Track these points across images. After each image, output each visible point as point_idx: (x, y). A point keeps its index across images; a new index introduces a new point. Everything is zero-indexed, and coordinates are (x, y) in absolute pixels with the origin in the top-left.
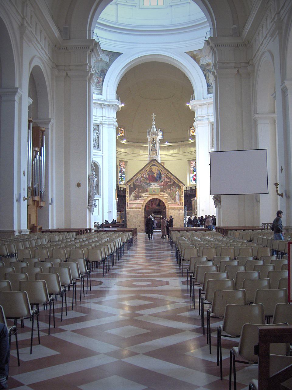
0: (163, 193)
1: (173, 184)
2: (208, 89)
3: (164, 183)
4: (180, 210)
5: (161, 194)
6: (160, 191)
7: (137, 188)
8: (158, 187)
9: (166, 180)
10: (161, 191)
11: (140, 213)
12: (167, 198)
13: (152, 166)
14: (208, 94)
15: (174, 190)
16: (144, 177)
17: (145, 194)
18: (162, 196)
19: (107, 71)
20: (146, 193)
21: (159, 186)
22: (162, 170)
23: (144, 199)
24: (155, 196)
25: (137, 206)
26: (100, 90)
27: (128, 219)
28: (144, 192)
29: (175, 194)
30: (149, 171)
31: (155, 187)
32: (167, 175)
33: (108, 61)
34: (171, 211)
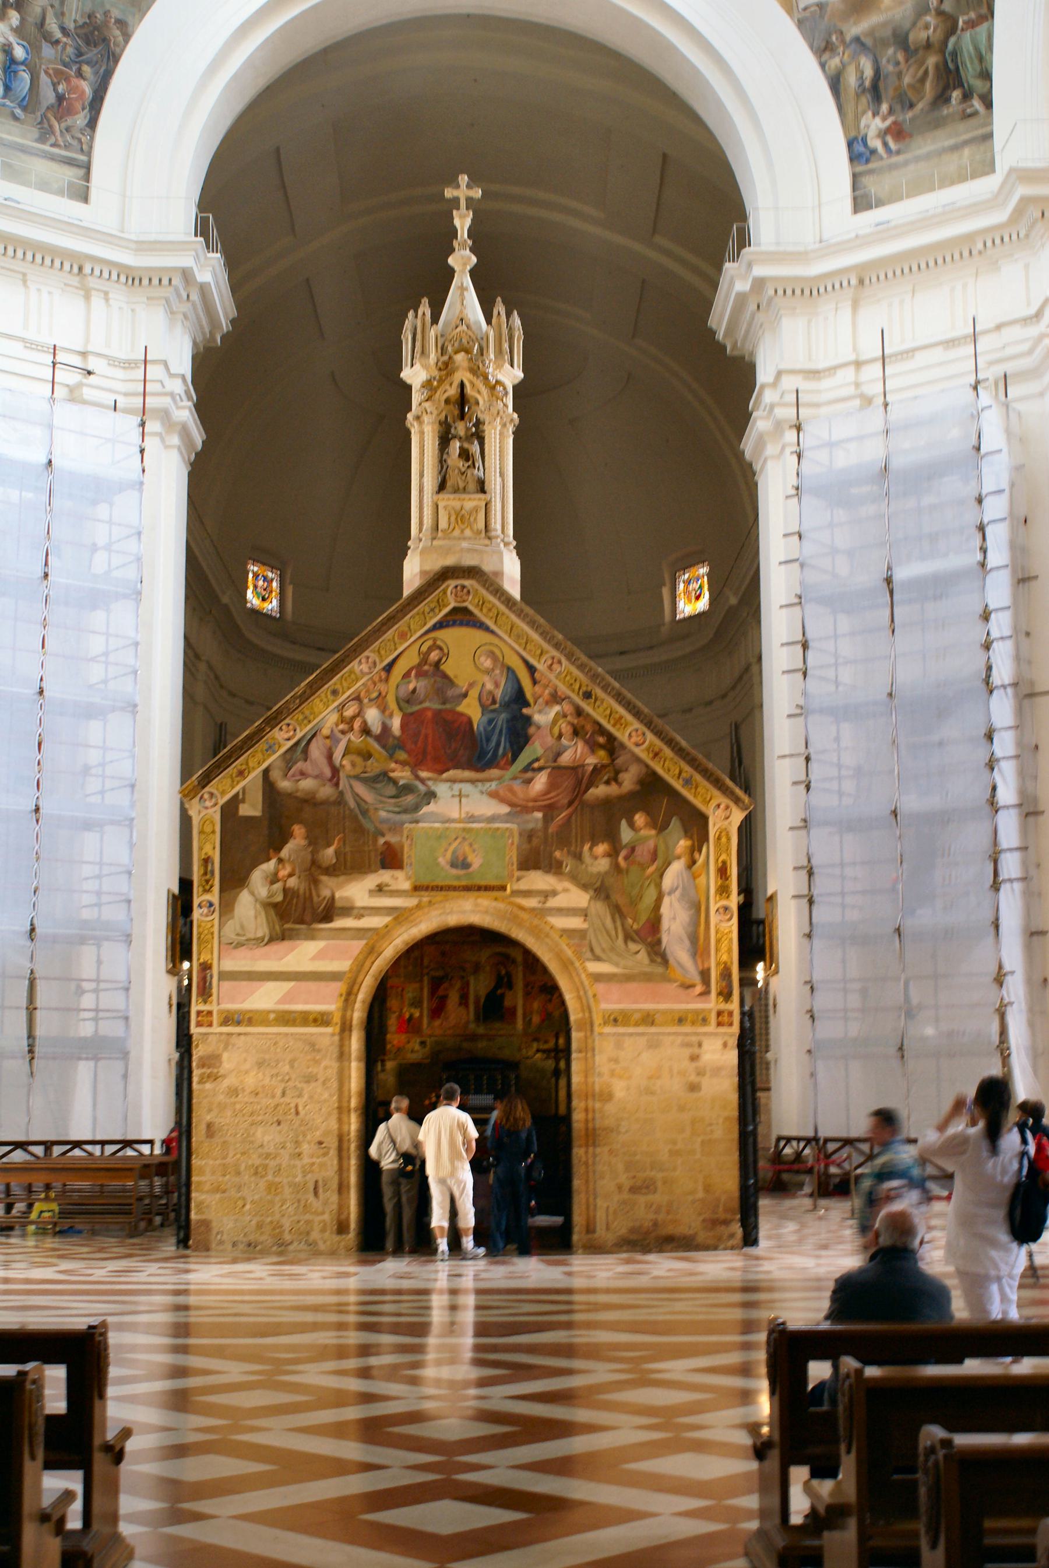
0: (538, 880)
1: (631, 795)
2: (855, 177)
3: (552, 785)
4: (706, 1046)
5: (523, 885)
6: (513, 856)
7: (298, 830)
8: (492, 819)
9: (574, 752)
10: (530, 861)
11: (328, 1066)
12: (575, 923)
13: (440, 626)
14: (861, 203)
15: (642, 853)
16: (366, 731)
17: (372, 881)
18: (532, 903)
19: (127, 37)
20: (385, 876)
21: (505, 809)
22: (531, 669)
23: (360, 933)
25: (286, 998)
26: (70, 162)
29: (659, 886)
31: (472, 818)
32: (579, 712)
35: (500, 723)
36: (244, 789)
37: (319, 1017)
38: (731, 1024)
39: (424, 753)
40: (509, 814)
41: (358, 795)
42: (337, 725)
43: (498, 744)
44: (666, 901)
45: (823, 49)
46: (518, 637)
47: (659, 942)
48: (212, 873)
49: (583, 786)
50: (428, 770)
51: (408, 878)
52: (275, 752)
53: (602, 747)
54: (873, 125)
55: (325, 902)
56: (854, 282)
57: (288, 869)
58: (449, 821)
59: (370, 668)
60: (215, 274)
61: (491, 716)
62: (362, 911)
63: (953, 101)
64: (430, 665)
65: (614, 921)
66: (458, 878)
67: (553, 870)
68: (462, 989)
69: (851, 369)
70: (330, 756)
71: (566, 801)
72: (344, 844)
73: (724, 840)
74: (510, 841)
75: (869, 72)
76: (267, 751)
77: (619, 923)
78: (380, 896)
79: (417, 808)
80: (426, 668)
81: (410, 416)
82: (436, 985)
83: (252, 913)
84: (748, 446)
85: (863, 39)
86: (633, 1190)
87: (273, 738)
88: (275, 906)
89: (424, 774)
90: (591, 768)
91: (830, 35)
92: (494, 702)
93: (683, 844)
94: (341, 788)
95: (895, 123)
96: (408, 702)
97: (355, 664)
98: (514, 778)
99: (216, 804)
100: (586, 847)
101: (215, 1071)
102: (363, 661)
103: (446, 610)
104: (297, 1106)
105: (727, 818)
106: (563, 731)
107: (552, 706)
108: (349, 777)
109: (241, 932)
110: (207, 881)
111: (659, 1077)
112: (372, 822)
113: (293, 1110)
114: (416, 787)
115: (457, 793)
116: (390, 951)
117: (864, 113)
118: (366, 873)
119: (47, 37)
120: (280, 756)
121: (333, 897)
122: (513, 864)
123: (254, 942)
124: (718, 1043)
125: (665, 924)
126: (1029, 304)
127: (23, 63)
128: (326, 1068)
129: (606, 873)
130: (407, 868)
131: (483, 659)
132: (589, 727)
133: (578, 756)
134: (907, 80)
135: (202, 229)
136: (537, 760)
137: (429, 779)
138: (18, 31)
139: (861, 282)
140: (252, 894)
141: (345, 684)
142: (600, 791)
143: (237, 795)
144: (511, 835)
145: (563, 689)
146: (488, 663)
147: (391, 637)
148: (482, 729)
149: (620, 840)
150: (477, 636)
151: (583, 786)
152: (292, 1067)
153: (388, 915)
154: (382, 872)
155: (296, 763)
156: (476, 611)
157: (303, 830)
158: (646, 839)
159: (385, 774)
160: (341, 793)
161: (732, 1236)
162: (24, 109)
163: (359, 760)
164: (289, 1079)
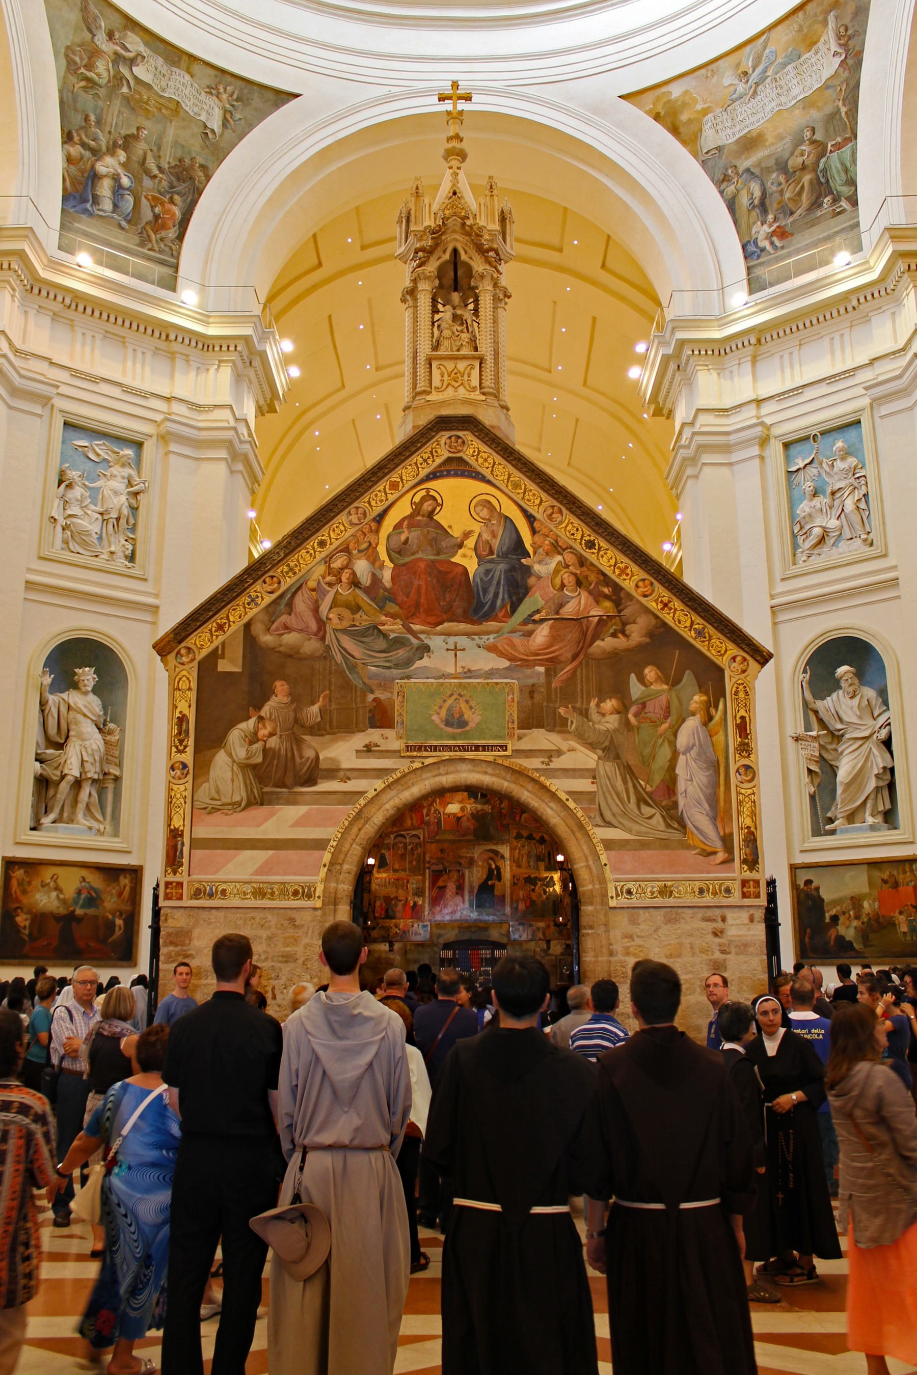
0: (541, 739)
1: (640, 648)
2: (749, 269)
3: (554, 638)
4: (730, 921)
5: (524, 745)
7: (281, 687)
8: (491, 673)
12: (583, 785)
13: (434, 476)
15: (654, 709)
16: (355, 583)
17: (359, 740)
19: (208, 178)
20: (374, 735)
21: (505, 663)
22: (530, 519)
28: (348, 727)
29: (673, 744)
30: (410, 521)
31: (469, 673)
32: (582, 562)
33: (215, 124)
34: (633, 921)
35: (497, 574)
36: (223, 644)
38: (758, 896)
39: (417, 605)
40: (507, 668)
41: (344, 649)
42: (324, 578)
43: (496, 595)
44: (682, 759)
45: (721, 182)
46: (516, 486)
47: (676, 804)
48: (187, 732)
52: (257, 605)
53: (606, 597)
54: (761, 231)
55: (308, 764)
56: (753, 341)
57: (269, 728)
58: (444, 676)
61: (489, 566)
62: (348, 774)
64: (423, 516)
65: (625, 782)
67: (557, 728)
68: (458, 881)
69: (754, 405)
70: (316, 610)
71: (569, 655)
72: (330, 701)
73: (742, 695)
74: (510, 698)
75: (757, 194)
76: (249, 604)
77: (630, 785)
78: (368, 758)
79: (409, 662)
80: (419, 518)
82: (436, 876)
85: (752, 170)
88: (254, 767)
89: (416, 627)
91: (727, 170)
92: (491, 552)
94: (327, 643)
95: (778, 227)
96: (399, 553)
97: (343, 517)
99: (192, 660)
100: (593, 704)
101: (185, 948)
102: (353, 511)
103: (438, 461)
105: (744, 671)
107: (553, 557)
108: (335, 630)
110: (181, 742)
111: (679, 956)
112: (361, 678)
114: (408, 640)
115: (453, 647)
117: (754, 223)
118: (353, 732)
119: (147, 172)
122: (513, 722)
125: (681, 785)
126: (896, 341)
127: (128, 189)
128: (306, 946)
129: (616, 730)
131: (479, 508)
132: (593, 577)
133: (582, 608)
134: (787, 195)
136: (538, 611)
137: (422, 632)
138: (125, 165)
139: (759, 341)
141: (332, 535)
142: (606, 644)
144: (512, 690)
145: (564, 537)
146: (485, 513)
147: (381, 488)
148: (478, 580)
150: (471, 487)
154: (370, 730)
155: (279, 617)
156: (472, 461)
157: (286, 687)
158: (658, 693)
159: (375, 627)
162: (129, 222)
163: (346, 613)
164: (266, 959)
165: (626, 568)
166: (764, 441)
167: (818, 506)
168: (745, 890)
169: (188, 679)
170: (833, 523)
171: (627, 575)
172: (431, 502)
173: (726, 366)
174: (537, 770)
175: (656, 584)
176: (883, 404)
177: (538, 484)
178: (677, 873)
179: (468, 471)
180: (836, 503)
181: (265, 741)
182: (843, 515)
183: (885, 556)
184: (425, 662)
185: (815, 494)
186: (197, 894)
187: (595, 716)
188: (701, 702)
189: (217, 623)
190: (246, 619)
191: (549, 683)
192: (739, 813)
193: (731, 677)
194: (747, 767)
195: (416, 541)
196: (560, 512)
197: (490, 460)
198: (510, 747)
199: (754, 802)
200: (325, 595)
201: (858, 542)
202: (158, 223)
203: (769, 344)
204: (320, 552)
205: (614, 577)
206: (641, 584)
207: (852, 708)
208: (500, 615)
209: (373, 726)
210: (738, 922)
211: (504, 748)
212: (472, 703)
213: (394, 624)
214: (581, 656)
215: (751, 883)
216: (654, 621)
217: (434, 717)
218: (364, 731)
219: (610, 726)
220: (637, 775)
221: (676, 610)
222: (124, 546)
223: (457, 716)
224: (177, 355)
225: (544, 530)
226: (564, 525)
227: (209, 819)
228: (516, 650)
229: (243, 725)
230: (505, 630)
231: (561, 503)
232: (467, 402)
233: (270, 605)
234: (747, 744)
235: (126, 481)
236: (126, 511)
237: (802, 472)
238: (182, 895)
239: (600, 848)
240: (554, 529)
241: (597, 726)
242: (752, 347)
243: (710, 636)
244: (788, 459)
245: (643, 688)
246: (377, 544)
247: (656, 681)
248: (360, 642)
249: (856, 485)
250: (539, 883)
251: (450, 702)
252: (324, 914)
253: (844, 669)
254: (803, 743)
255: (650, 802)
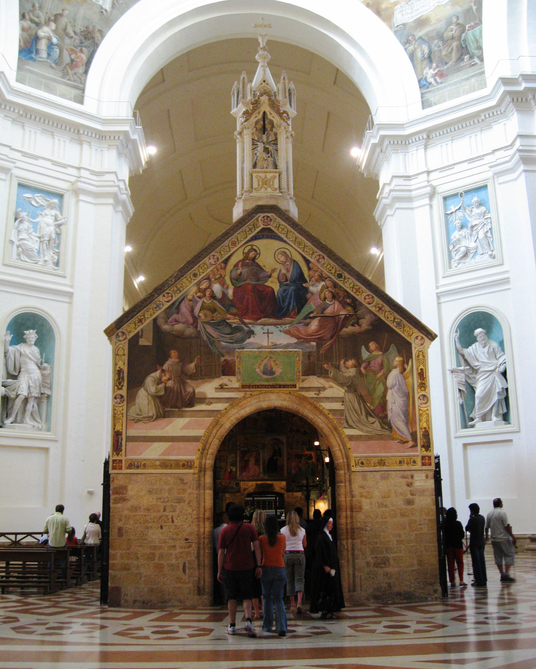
0: (314, 381)
1: (367, 332)
2: (422, 95)
3: (321, 327)
4: (416, 478)
5: (306, 385)
7: (174, 353)
8: (287, 346)
11: (190, 493)
12: (337, 406)
13: (255, 238)
14: (425, 104)
15: (375, 365)
16: (213, 296)
17: (217, 382)
18: (311, 394)
19: (103, 37)
20: (225, 380)
21: (294, 340)
22: (307, 262)
24: (273, 397)
27: (120, 529)
30: (243, 263)
31: (275, 346)
32: (335, 285)
34: (365, 478)
35: (290, 292)
36: (142, 330)
37: (186, 463)
38: (430, 465)
41: (207, 332)
42: (196, 294)
43: (289, 303)
44: (389, 392)
45: (406, 43)
46: (300, 244)
47: (386, 416)
49: (339, 326)
50: (249, 319)
51: (238, 381)
52: (160, 309)
53: (349, 304)
54: (429, 73)
56: (425, 137)
57: (168, 376)
59: (215, 262)
60: (139, 136)
63: (465, 60)
64: (249, 260)
65: (359, 405)
66: (267, 380)
69: (425, 175)
70: (192, 311)
71: (329, 336)
73: (421, 357)
74: (297, 359)
75: (426, 51)
79: (243, 340)
80: (247, 261)
81: (236, 133)
82: (244, 453)
83: (146, 402)
84: (377, 214)
85: (423, 37)
86: (376, 565)
87: (159, 301)
88: (160, 397)
89: (247, 321)
90: (343, 316)
91: (409, 37)
92: (287, 280)
93: (398, 359)
95: (439, 71)
96: (237, 280)
97: (206, 260)
98: (299, 323)
99: (125, 339)
100: (342, 362)
101: (124, 496)
103: (258, 230)
104: (172, 517)
105: (422, 344)
106: (327, 296)
107: (320, 282)
109: (139, 413)
110: (120, 383)
111: (389, 497)
113: (170, 520)
114: (242, 328)
116: (228, 424)
117: (425, 68)
119: (67, 35)
120: (163, 311)
121: (194, 392)
122: (299, 372)
123: (147, 419)
124: (423, 475)
125: (389, 406)
127: (56, 45)
128: (190, 494)
129: (354, 377)
130: (238, 375)
131: (280, 256)
132: (341, 294)
134: (444, 53)
135: (135, 115)
136: (312, 312)
137: (250, 323)
138: (55, 32)
139: (428, 137)
140: (147, 391)
141: (201, 271)
142: (349, 329)
143: (138, 333)
145: (326, 272)
146: (283, 259)
147: (227, 244)
148: (280, 295)
149: (361, 358)
150: (277, 244)
151: (339, 326)
152: (169, 494)
153: (227, 402)
155: (172, 315)
157: (177, 353)
158: (377, 356)
160: (199, 332)
161: (436, 591)
162: (56, 64)
164: (168, 501)
165: (359, 288)
166: (432, 196)
167: (464, 234)
168: (423, 461)
169: (123, 349)
170: (472, 245)
171: (360, 292)
172: (253, 252)
173: (409, 151)
174: (312, 398)
175: (376, 298)
176: (500, 176)
177: (312, 243)
178: (387, 452)
179: (274, 236)
180: (474, 233)
181: (166, 383)
182: (478, 241)
183: (502, 264)
184: (251, 340)
185: (462, 227)
186: (130, 466)
187: (343, 369)
188: (400, 361)
189: (139, 319)
190: (154, 316)
191: (318, 352)
192: (420, 420)
193: (415, 348)
194: (424, 396)
195: (246, 274)
196: (323, 258)
197: (286, 230)
198: (297, 386)
199: (428, 414)
200: (197, 303)
201: (486, 256)
202: (73, 64)
203: (435, 139)
204: (194, 280)
205: (352, 293)
206: (367, 297)
207: (484, 353)
208: (292, 314)
209: (224, 375)
210: (420, 478)
211: (295, 386)
212: (277, 362)
213: (236, 319)
214: (335, 337)
215: (427, 458)
216: (374, 317)
217: (257, 370)
218: (219, 377)
219: (351, 374)
220: (366, 400)
221: (386, 311)
222: (52, 257)
223: (269, 369)
224: (84, 142)
225: (315, 268)
226: (325, 265)
227: (136, 425)
228: (301, 333)
229: (153, 375)
230: (294, 323)
231: (324, 253)
232: (272, 197)
233: (167, 309)
234: (424, 384)
235: (54, 218)
236: (54, 236)
237: (454, 214)
238: (122, 467)
239: (346, 439)
240: (320, 267)
241: (344, 374)
242: (424, 141)
243: (404, 325)
244: (445, 207)
245: (368, 353)
246: (225, 275)
247: (375, 350)
248: (217, 329)
249: (485, 222)
250: (304, 458)
251: (265, 361)
252: (199, 477)
253: (478, 331)
254: (456, 373)
255: (372, 414)
